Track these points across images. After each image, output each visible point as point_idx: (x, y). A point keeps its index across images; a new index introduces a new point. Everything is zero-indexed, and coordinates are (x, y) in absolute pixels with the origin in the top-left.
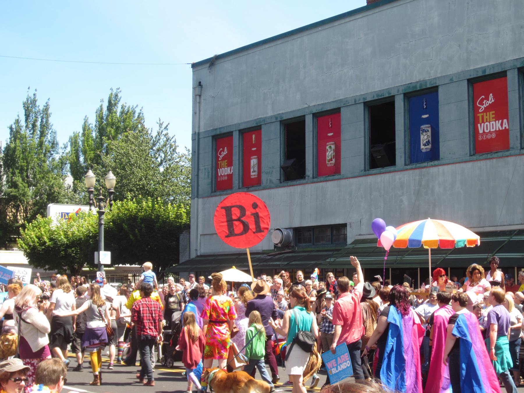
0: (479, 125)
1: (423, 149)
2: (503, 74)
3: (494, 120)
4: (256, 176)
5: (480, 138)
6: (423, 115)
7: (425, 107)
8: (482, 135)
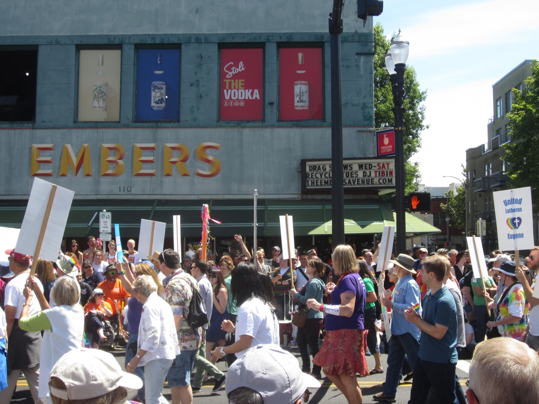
0: (225, 91)
1: (154, 107)
2: (261, 45)
3: (244, 88)
4: (307, 108)
5: (226, 104)
6: (156, 70)
7: (159, 62)
8: (229, 102)
